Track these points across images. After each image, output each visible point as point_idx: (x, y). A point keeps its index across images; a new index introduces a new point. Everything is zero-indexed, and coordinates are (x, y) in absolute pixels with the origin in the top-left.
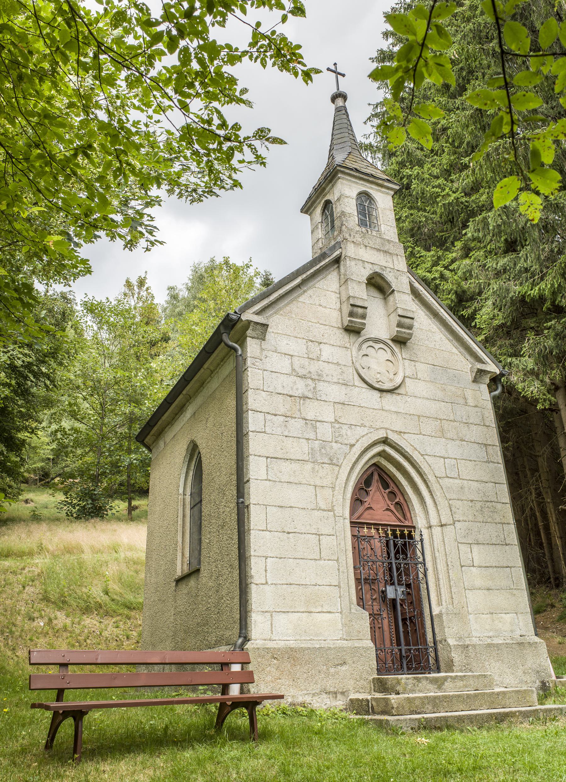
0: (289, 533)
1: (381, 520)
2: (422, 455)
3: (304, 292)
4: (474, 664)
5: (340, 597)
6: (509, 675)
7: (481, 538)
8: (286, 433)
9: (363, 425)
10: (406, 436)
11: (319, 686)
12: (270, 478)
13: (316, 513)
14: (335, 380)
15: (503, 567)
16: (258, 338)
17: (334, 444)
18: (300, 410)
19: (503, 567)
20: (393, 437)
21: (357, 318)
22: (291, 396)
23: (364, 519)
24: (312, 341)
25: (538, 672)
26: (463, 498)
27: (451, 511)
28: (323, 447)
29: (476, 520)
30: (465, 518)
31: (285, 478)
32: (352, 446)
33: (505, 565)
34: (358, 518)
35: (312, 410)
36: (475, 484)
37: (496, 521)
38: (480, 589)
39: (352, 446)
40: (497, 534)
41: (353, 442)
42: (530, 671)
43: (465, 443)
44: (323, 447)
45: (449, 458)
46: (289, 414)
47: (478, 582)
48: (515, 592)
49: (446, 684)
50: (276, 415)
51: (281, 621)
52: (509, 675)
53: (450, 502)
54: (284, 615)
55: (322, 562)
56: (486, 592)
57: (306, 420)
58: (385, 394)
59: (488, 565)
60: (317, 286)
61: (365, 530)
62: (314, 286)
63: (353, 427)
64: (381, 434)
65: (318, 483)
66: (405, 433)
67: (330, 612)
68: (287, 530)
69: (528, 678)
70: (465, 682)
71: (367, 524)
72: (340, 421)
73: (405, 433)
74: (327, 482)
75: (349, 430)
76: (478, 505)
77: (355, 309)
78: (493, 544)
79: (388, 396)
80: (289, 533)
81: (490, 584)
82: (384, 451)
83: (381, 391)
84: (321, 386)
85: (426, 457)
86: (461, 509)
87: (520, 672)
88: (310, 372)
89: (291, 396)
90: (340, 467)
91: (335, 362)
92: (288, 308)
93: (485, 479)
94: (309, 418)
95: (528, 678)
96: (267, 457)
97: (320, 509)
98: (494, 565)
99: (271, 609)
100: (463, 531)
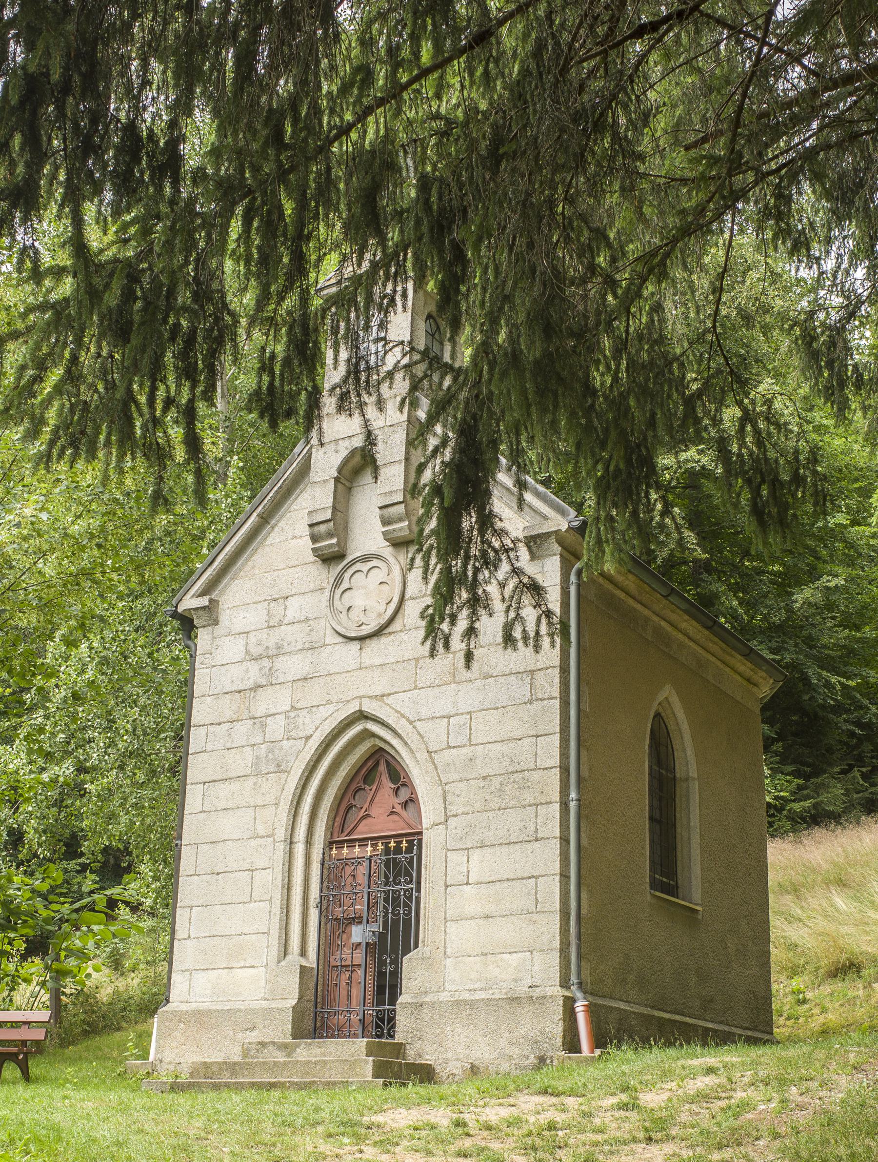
0: (218, 874)
1: (383, 831)
2: (411, 723)
3: (273, 528)
4: (428, 1030)
5: (268, 947)
6: (482, 1045)
7: (490, 837)
8: (228, 745)
9: (329, 702)
10: (390, 700)
11: (222, 1054)
12: (205, 809)
13: (253, 843)
14: (299, 647)
15: (523, 879)
16: (209, 625)
17: (285, 742)
18: (248, 708)
19: (523, 879)
20: (369, 707)
21: (323, 540)
22: (240, 692)
23: (362, 833)
24: (275, 600)
25: (536, 1042)
26: (470, 777)
27: (445, 802)
28: (271, 751)
29: (487, 808)
30: (468, 809)
31: (222, 805)
32: (308, 738)
33: (526, 875)
34: (349, 834)
35: (262, 704)
36: (498, 747)
37: (524, 803)
38: (472, 918)
39: (308, 738)
40: (522, 824)
41: (309, 732)
42: (522, 1041)
43: (491, 680)
44: (271, 751)
45: (457, 714)
46: (235, 717)
47: (471, 908)
48: (535, 917)
49: (298, 1050)
50: (219, 724)
51: (201, 979)
52: (482, 1045)
53: (447, 788)
54: (203, 973)
55: (252, 905)
56: (482, 922)
57: (255, 718)
58: (368, 641)
59: (494, 878)
60: (292, 509)
61: (357, 849)
62: (288, 511)
63: (314, 709)
64: (353, 708)
65: (260, 802)
66: (389, 694)
67: (253, 967)
68: (217, 870)
69: (515, 1051)
70: (323, 1050)
71: (372, 839)
72: (298, 706)
73: (389, 694)
74: (270, 799)
75: (308, 716)
76: (496, 782)
77: (316, 529)
78: (510, 843)
79: (373, 644)
80: (218, 874)
81: (492, 908)
82: (366, 730)
83: (378, 633)
84: (281, 663)
85: (418, 724)
86: (464, 794)
87: (503, 1043)
88: (267, 648)
89: (240, 692)
90: (289, 773)
91: (303, 618)
92: (250, 563)
93: (517, 734)
94: (258, 715)
95: (515, 1051)
96: (204, 783)
97: (258, 837)
98: (505, 877)
99: (191, 968)
100: (459, 831)
